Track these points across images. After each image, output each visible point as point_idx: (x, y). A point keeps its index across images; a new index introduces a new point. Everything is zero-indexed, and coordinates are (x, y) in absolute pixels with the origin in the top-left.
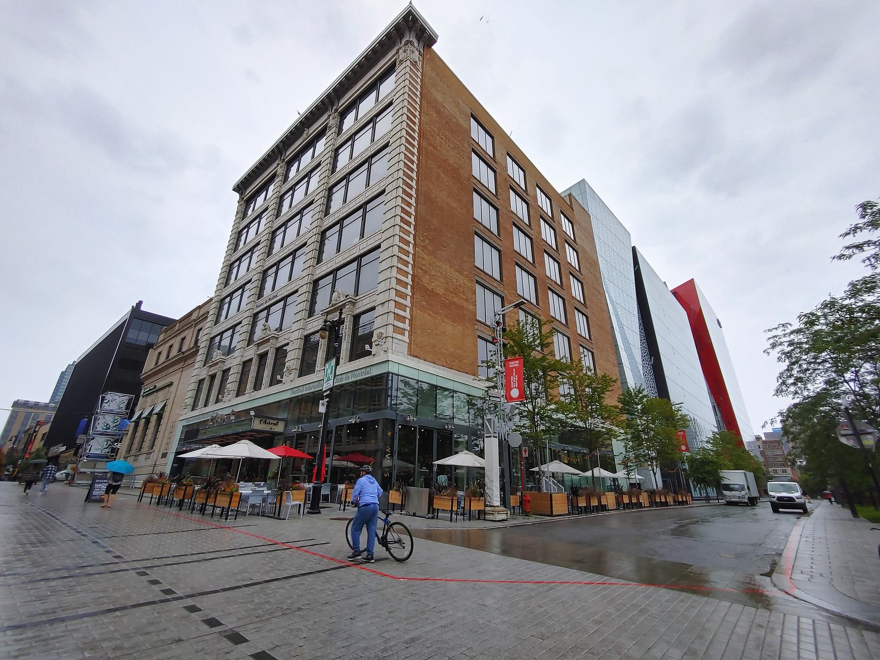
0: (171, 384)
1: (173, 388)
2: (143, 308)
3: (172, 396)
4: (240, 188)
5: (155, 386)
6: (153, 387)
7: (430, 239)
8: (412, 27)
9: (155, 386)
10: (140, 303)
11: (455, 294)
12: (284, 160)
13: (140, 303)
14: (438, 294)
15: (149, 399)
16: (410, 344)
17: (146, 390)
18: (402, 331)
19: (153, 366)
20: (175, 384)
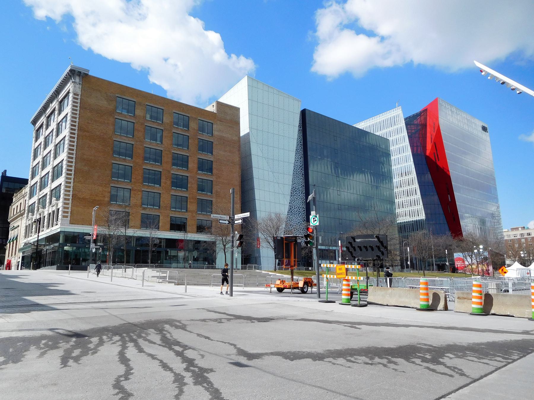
0: (18, 226)
1: (19, 228)
2: (8, 174)
3: (20, 232)
4: (34, 122)
5: (14, 226)
6: (13, 227)
7: (82, 177)
8: (74, 73)
9: (14, 226)
10: (5, 171)
11: (97, 196)
12: (46, 116)
13: (5, 171)
14: (86, 199)
15: (13, 231)
16: (70, 220)
17: (11, 228)
18: (67, 217)
19: (12, 216)
20: (20, 226)
